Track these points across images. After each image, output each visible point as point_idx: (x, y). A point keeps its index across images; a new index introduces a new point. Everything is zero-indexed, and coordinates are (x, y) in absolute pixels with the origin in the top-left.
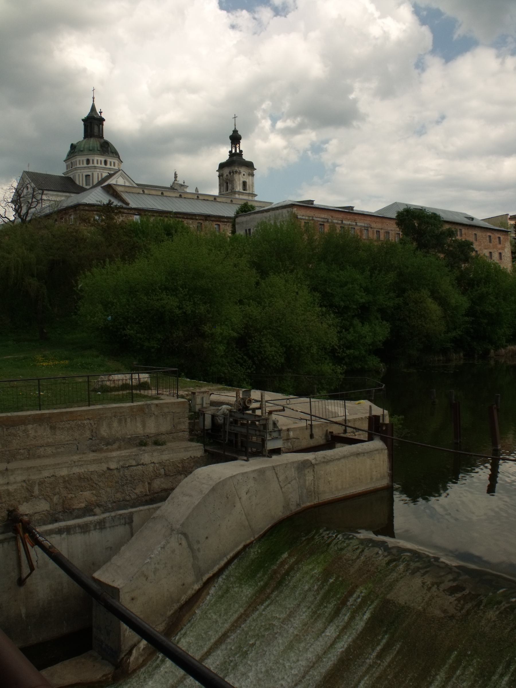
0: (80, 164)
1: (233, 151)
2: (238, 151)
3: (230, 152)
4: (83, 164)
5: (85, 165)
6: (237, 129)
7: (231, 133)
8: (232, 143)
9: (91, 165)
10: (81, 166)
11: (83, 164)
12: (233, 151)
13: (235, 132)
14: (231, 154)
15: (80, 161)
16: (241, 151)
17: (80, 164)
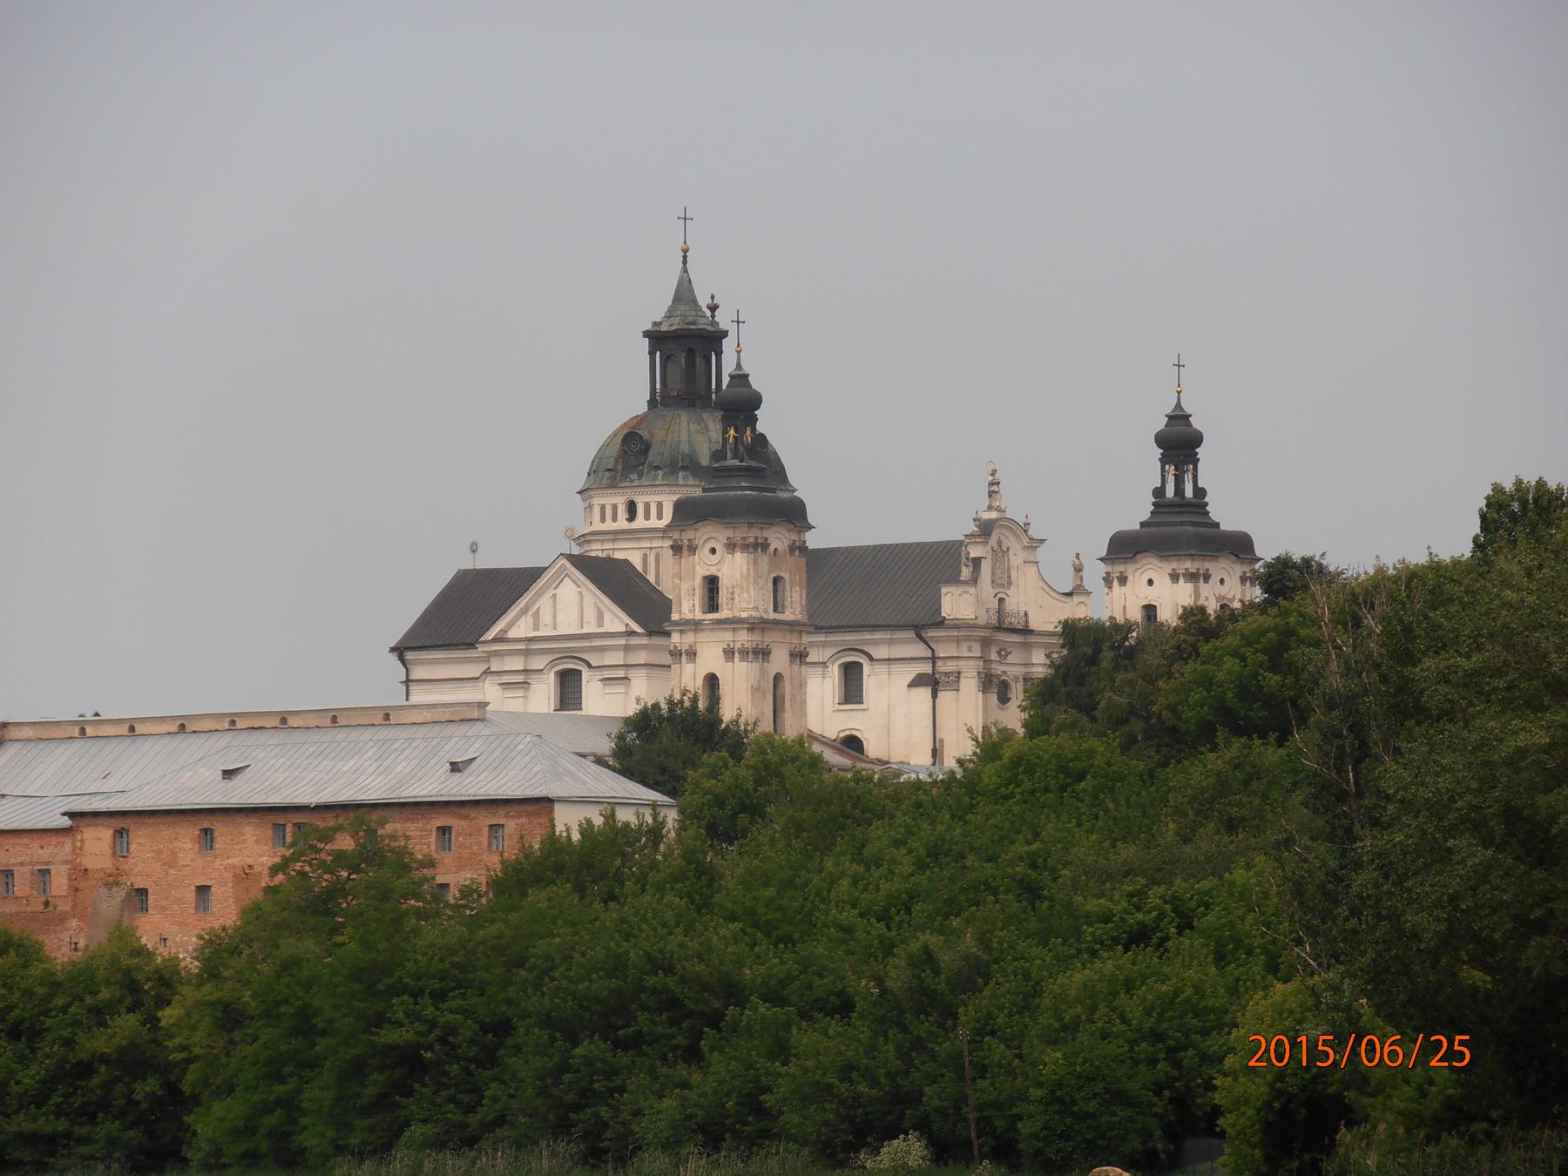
0: (603, 520)
1: (1170, 492)
2: (1189, 493)
3: (1159, 492)
4: (615, 519)
5: (622, 523)
6: (1188, 409)
7: (1161, 423)
8: (1164, 460)
9: (639, 522)
10: (609, 525)
11: (615, 519)
12: (1170, 492)
13: (1179, 418)
14: (1161, 504)
15: (603, 508)
16: (1200, 493)
17: (603, 520)
